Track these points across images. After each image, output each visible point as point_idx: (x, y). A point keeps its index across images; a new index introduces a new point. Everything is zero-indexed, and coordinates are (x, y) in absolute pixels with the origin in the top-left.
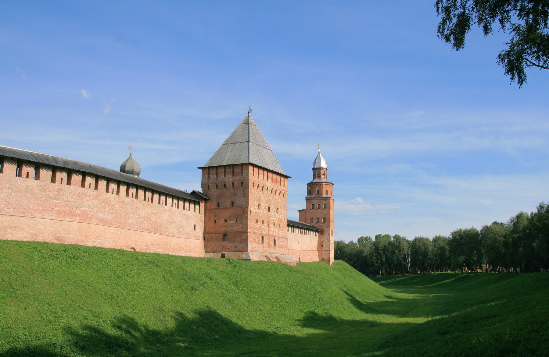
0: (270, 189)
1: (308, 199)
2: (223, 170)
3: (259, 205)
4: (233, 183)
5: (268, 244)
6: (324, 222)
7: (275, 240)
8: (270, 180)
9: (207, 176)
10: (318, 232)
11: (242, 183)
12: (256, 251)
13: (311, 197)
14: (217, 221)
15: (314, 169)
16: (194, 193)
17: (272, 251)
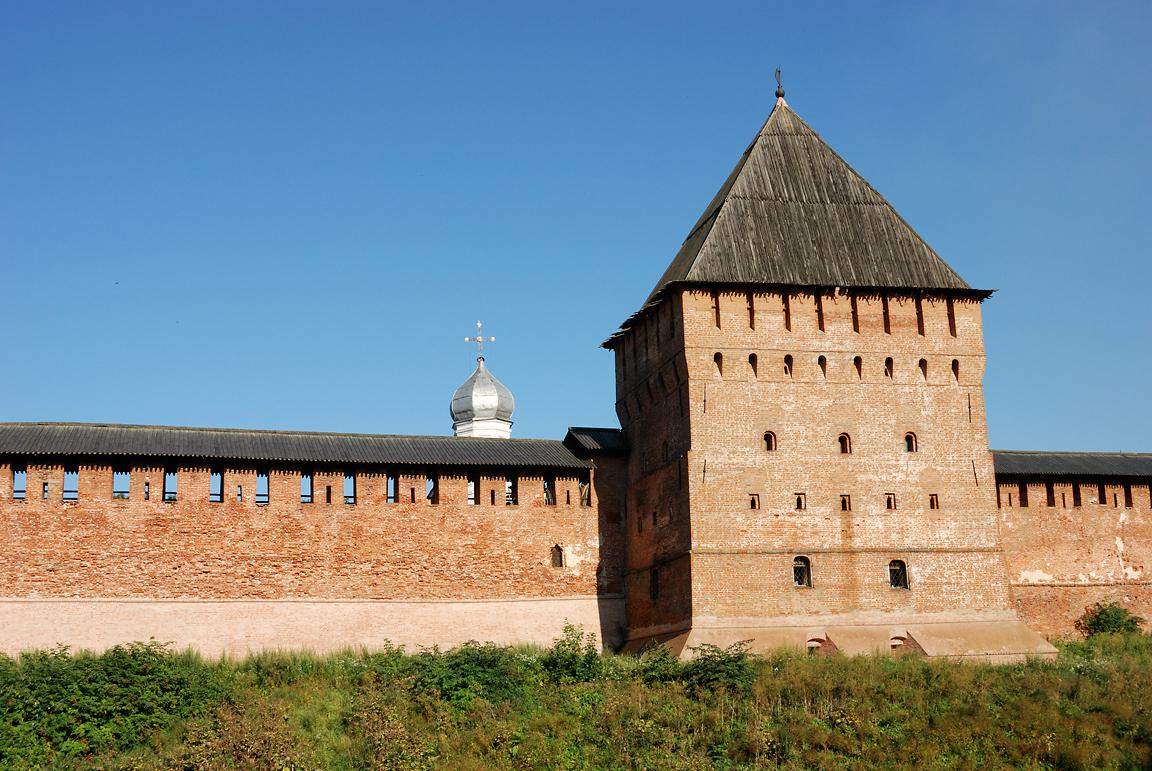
12: (714, 625)
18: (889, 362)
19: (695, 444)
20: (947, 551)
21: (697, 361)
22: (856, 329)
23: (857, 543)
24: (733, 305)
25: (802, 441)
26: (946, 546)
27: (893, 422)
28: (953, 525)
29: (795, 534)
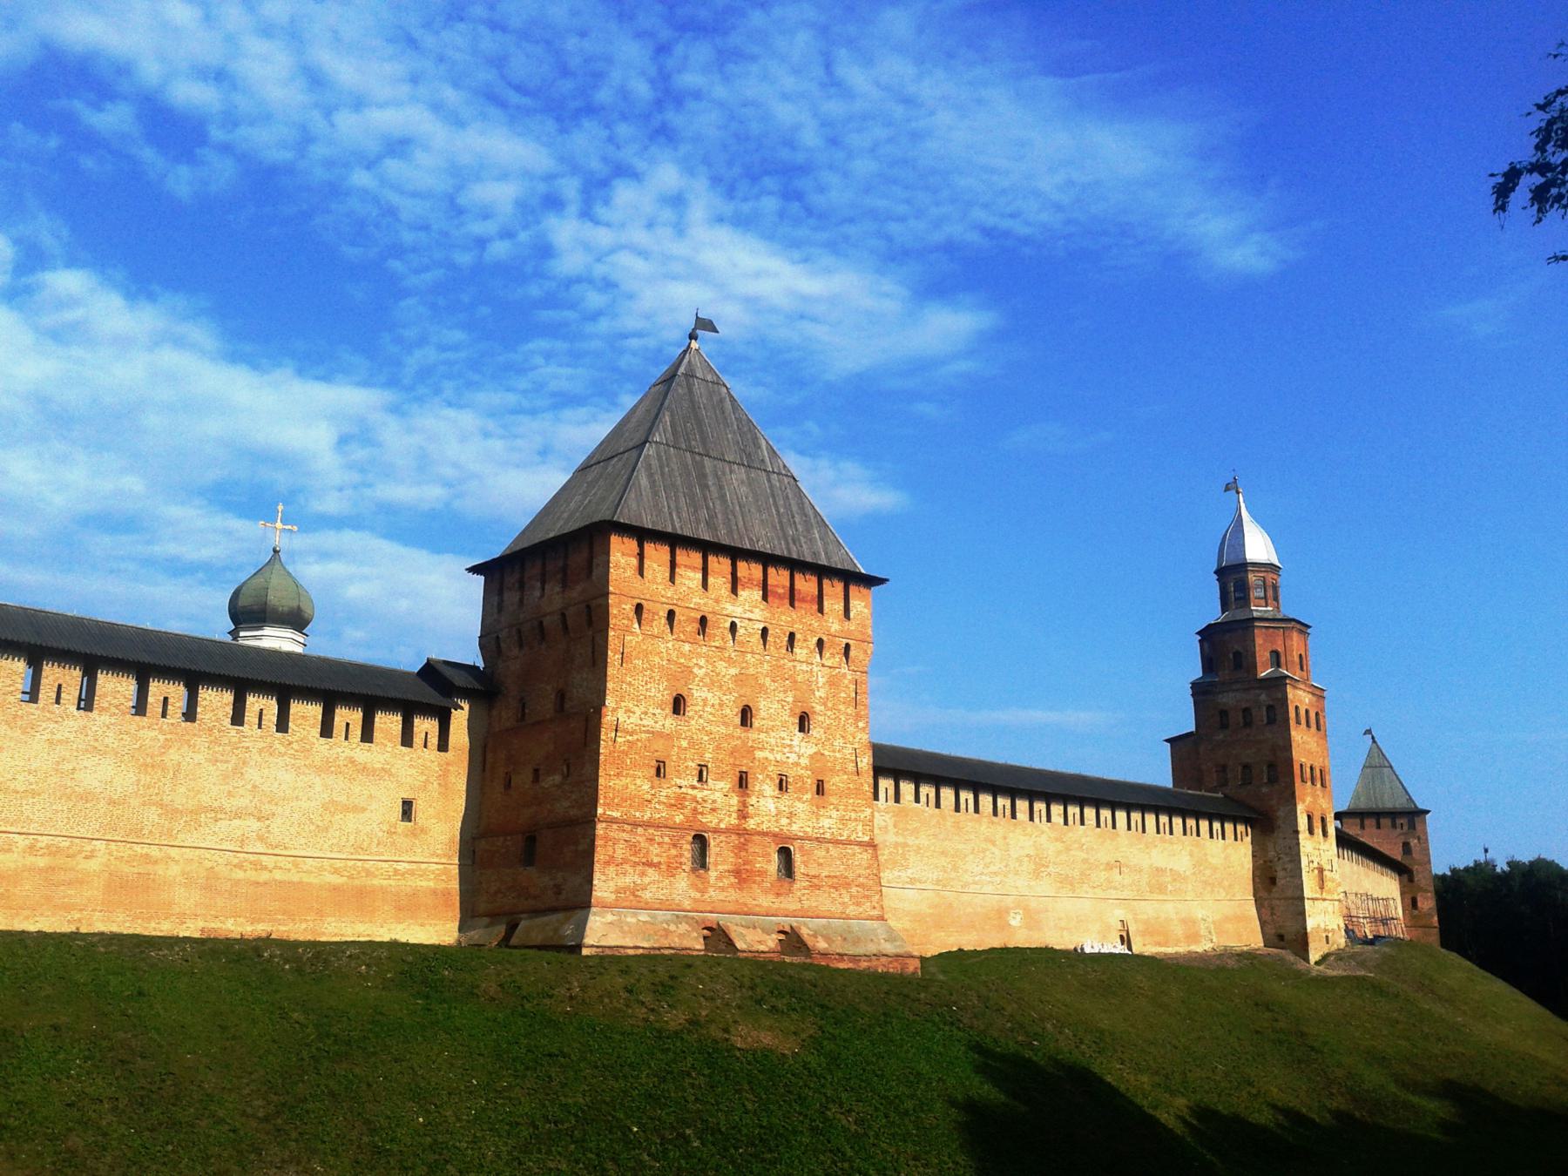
0: (749, 632)
1: (1200, 691)
4: (563, 615)
5: (737, 873)
6: (1272, 780)
8: (751, 595)
10: (1247, 821)
13: (1212, 684)
15: (1221, 572)
16: (432, 672)
17: (766, 901)
18: (792, 636)
19: (610, 701)
20: (829, 842)
21: (619, 610)
22: (765, 598)
23: (751, 824)
24: (657, 556)
25: (708, 709)
26: (828, 836)
27: (790, 699)
28: (834, 814)
29: (695, 809)
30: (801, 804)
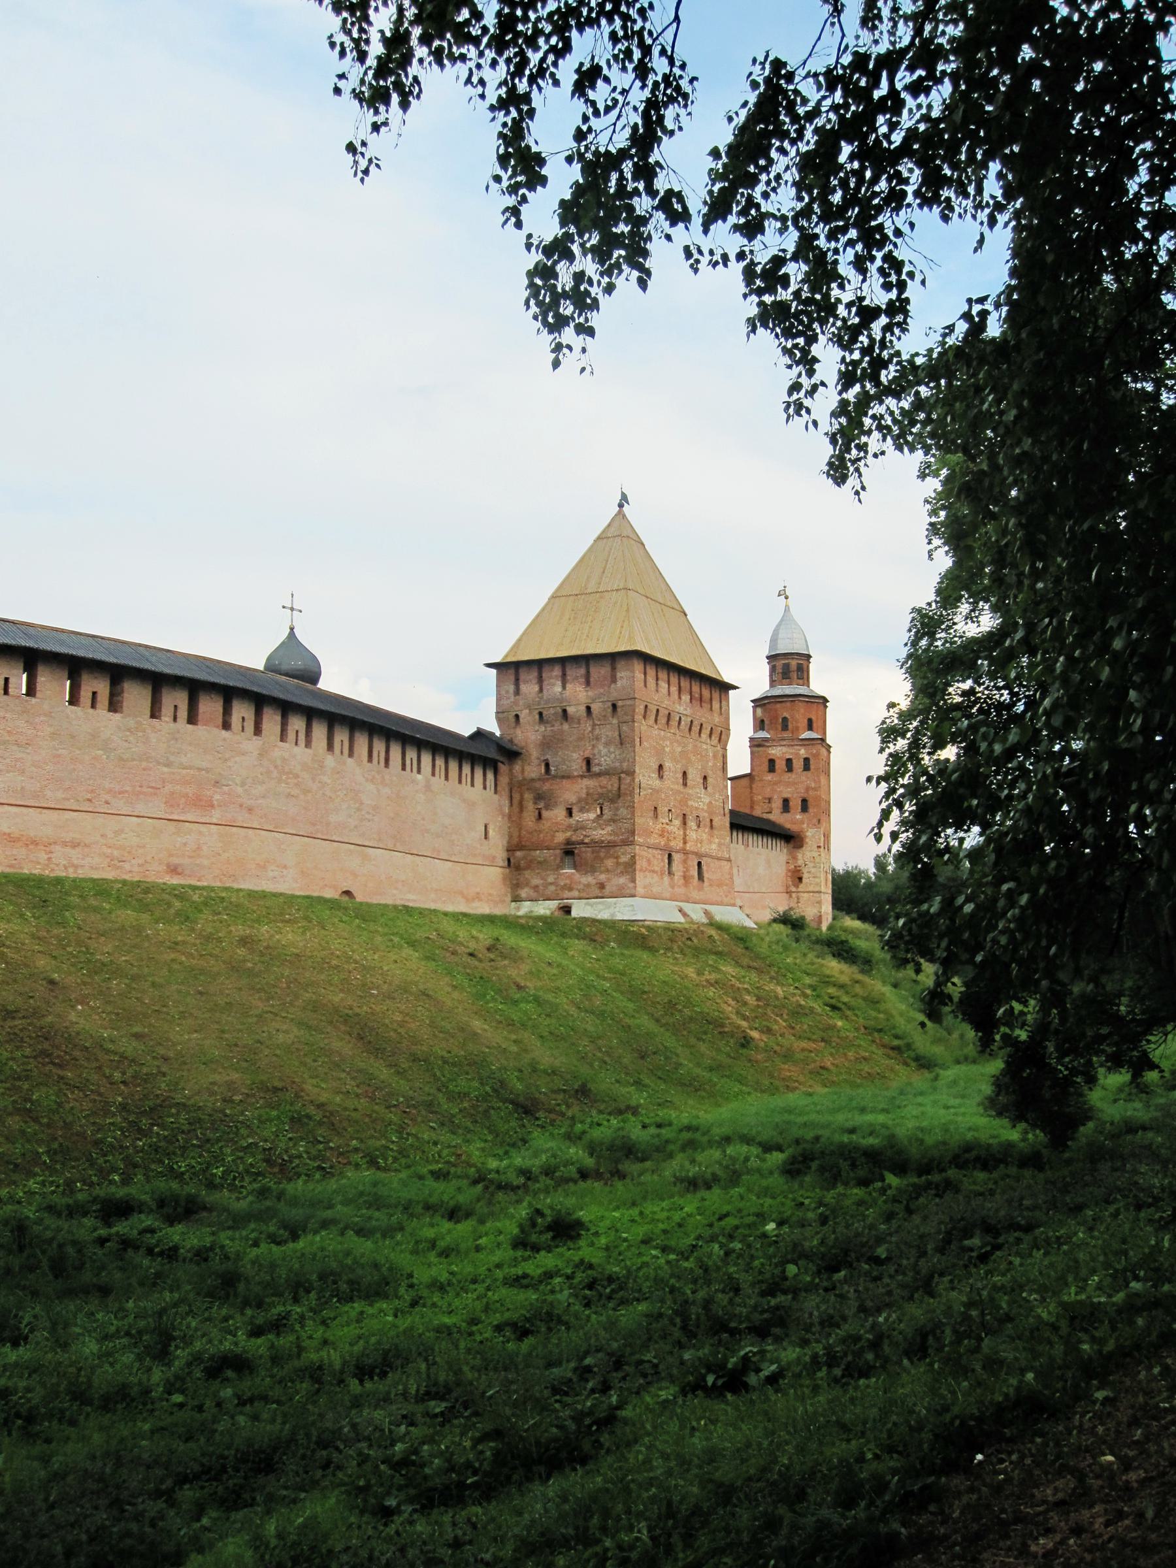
2: (557, 671)
3: (661, 767)
4: (588, 708)
7: (699, 864)
8: (686, 698)
9: (512, 688)
11: (614, 706)
13: (766, 740)
14: (545, 814)
16: (479, 735)
30: (704, 833)
